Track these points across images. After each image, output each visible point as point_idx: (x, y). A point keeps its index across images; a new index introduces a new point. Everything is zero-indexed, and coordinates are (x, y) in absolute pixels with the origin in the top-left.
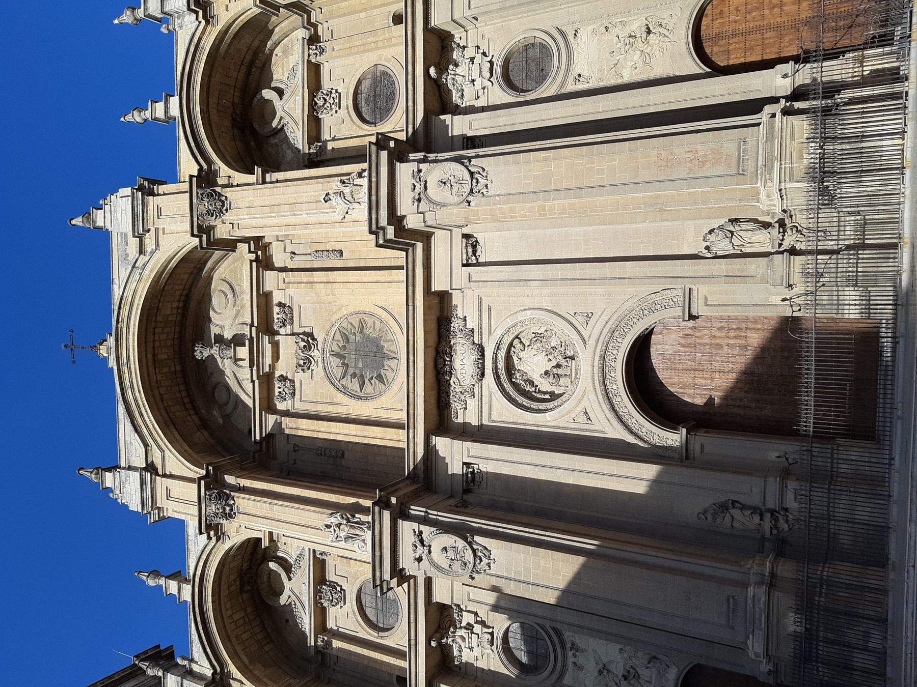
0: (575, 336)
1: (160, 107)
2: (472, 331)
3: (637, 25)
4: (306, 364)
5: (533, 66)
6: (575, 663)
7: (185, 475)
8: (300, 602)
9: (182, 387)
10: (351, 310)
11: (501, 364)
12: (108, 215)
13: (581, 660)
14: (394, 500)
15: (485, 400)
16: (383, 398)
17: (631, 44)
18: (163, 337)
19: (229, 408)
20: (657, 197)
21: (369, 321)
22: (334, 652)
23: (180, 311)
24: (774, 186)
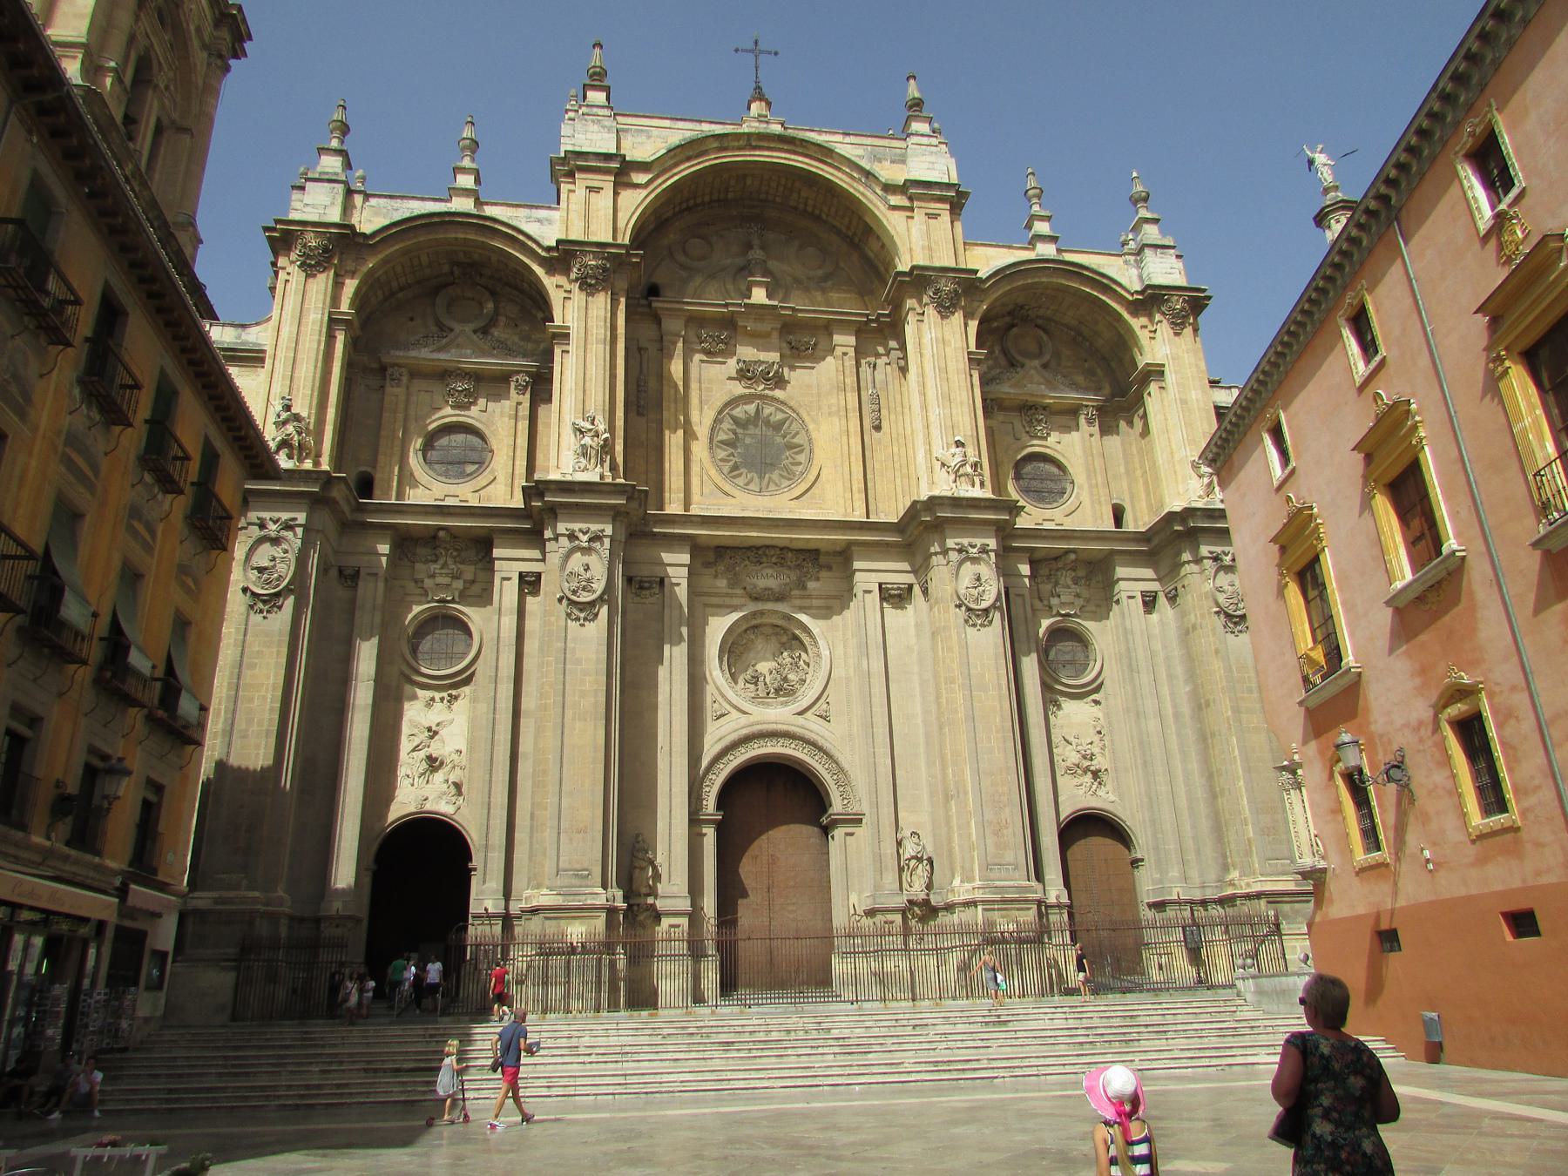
0: (805, 703)
1: (1042, 228)
2: (805, 588)
3: (1100, 762)
4: (745, 374)
5: (1068, 657)
6: (433, 699)
7: (620, 215)
8: (447, 344)
9: (707, 199)
10: (814, 435)
11: (765, 620)
12: (925, 140)
13: (438, 705)
14: (634, 504)
15: (728, 601)
16: (713, 472)
17: (1084, 757)
18: (774, 184)
19: (682, 259)
20: (966, 793)
21: (802, 458)
22: (388, 389)
23: (801, 206)
24: (978, 895)
